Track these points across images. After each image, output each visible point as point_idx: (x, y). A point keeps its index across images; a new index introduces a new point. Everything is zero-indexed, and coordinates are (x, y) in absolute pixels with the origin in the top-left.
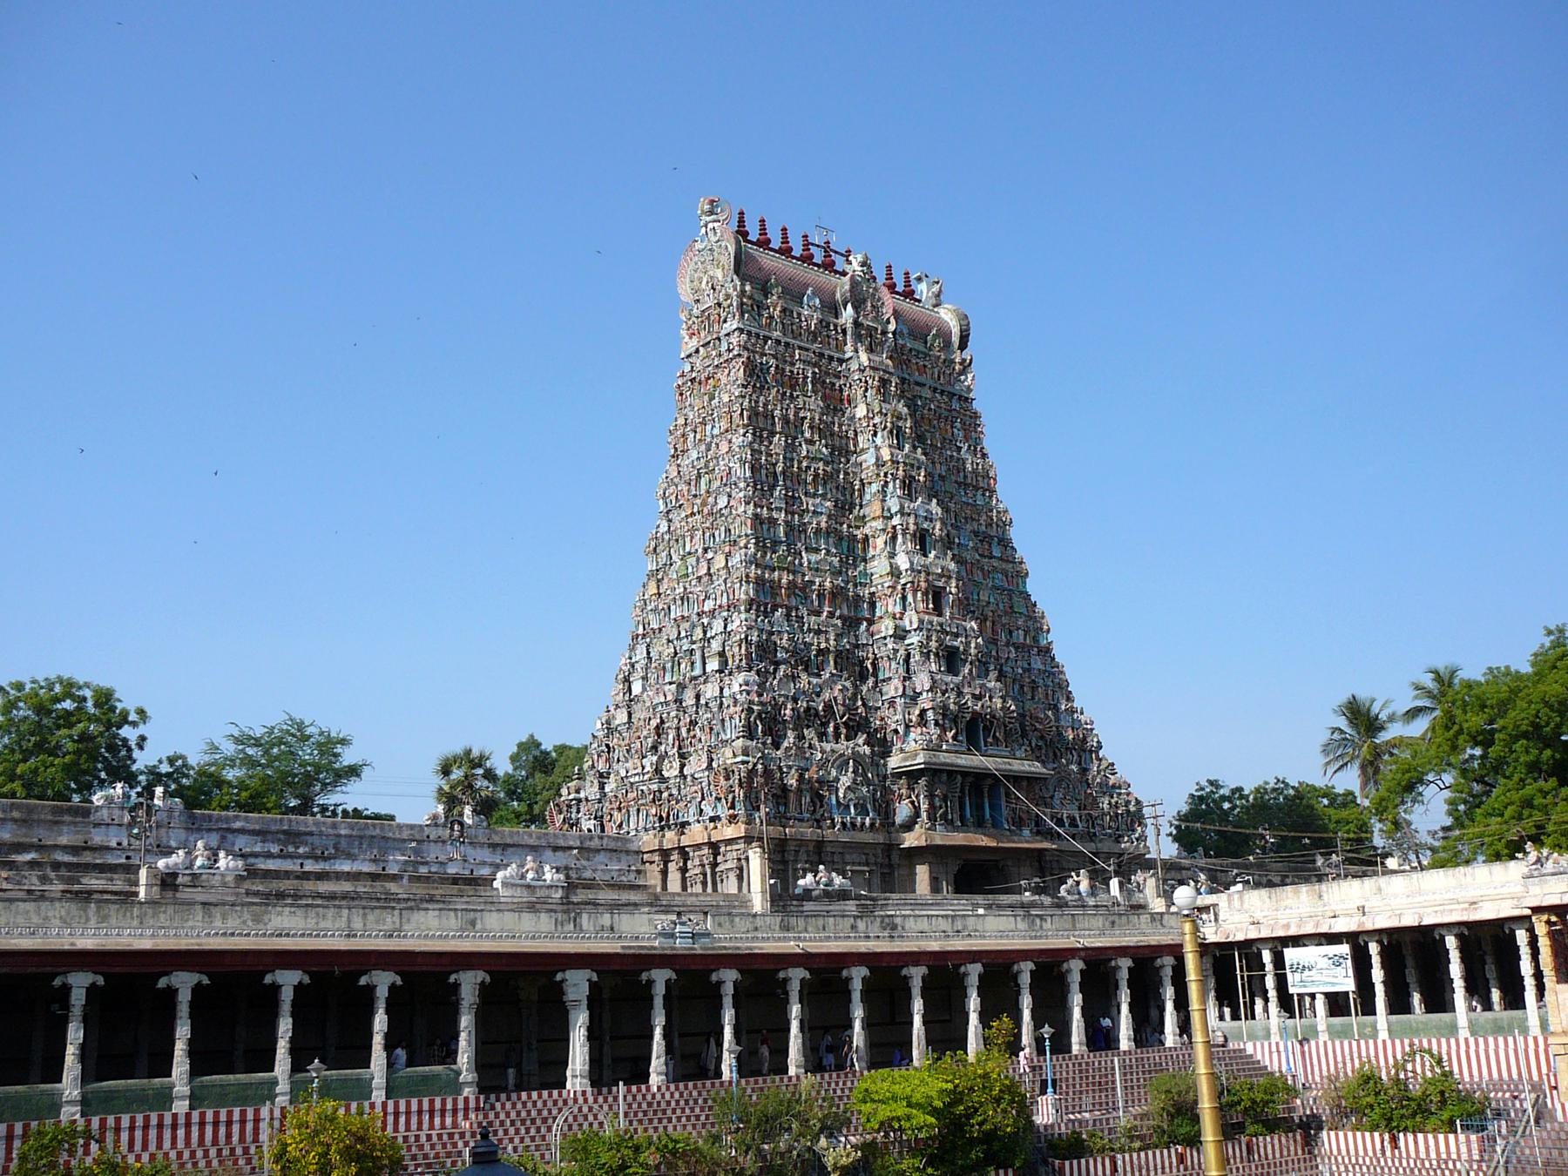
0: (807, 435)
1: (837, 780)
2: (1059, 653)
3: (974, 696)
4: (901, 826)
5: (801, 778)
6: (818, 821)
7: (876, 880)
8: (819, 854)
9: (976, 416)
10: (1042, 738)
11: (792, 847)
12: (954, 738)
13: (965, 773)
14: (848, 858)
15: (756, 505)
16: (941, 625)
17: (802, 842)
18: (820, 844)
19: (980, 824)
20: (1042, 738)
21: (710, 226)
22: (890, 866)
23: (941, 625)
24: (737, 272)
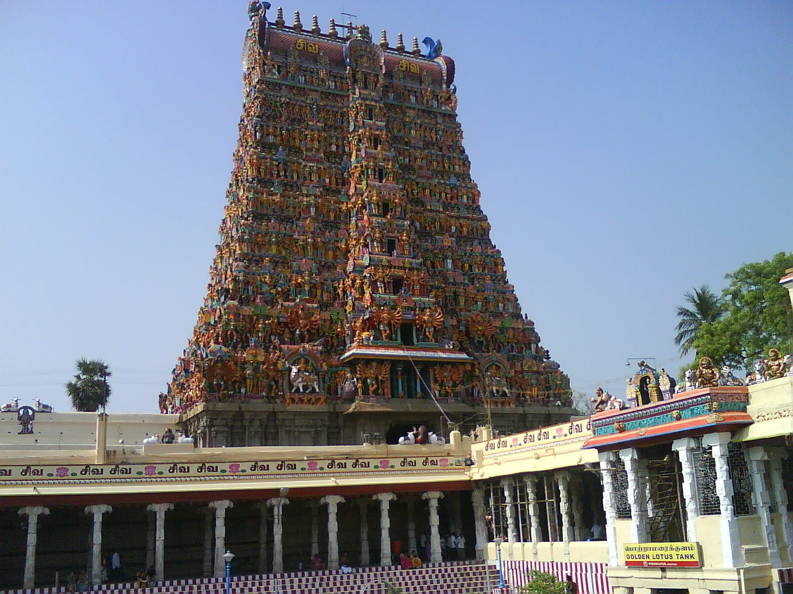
0: (309, 146)
1: (290, 370)
2: (511, 279)
3: (409, 308)
4: (345, 400)
5: (256, 369)
6: (274, 398)
7: (324, 437)
8: (275, 420)
9: (459, 126)
10: (483, 335)
11: (247, 416)
12: (389, 337)
13: (394, 362)
14: (297, 423)
15: (256, 192)
16: (389, 262)
17: (256, 413)
18: (273, 414)
19: (410, 394)
20: (483, 335)
21: (253, 19)
22: (338, 427)
23: (389, 262)
24: (261, 44)
